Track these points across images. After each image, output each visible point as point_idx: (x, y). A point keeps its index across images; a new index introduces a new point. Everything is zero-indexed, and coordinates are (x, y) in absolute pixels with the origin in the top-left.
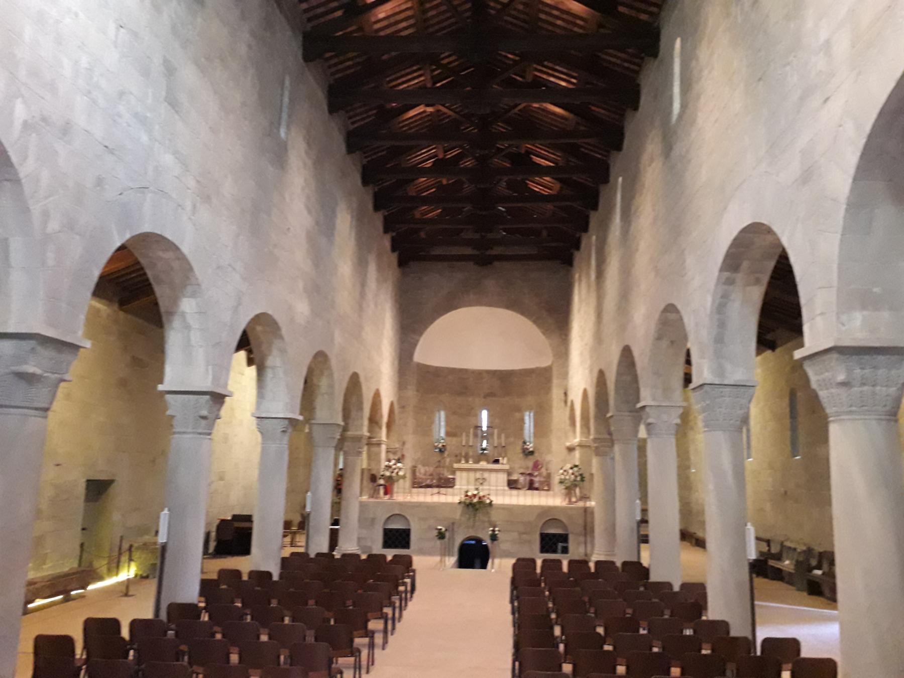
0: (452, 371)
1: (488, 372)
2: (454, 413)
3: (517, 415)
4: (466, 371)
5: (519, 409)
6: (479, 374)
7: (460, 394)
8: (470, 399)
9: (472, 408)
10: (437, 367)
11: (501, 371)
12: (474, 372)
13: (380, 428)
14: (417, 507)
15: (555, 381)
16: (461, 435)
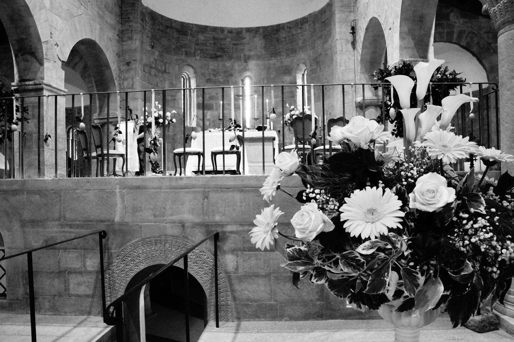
0: (203, 29)
1: (249, 30)
2: (208, 81)
3: (287, 78)
4: (222, 30)
5: (289, 71)
6: (238, 34)
7: (215, 57)
8: (228, 64)
9: (231, 75)
10: (182, 24)
11: (265, 28)
12: (231, 31)
13: (42, 64)
14: (15, 192)
15: (338, 16)
16: (217, 109)
